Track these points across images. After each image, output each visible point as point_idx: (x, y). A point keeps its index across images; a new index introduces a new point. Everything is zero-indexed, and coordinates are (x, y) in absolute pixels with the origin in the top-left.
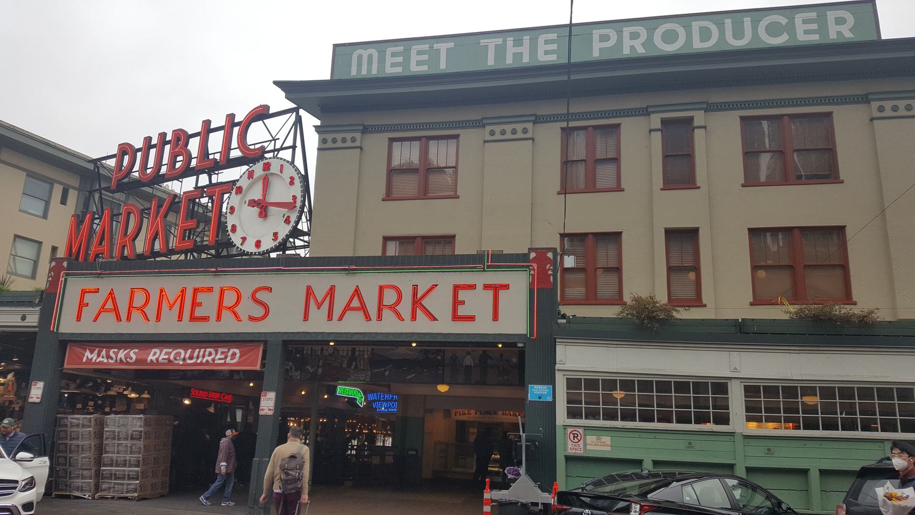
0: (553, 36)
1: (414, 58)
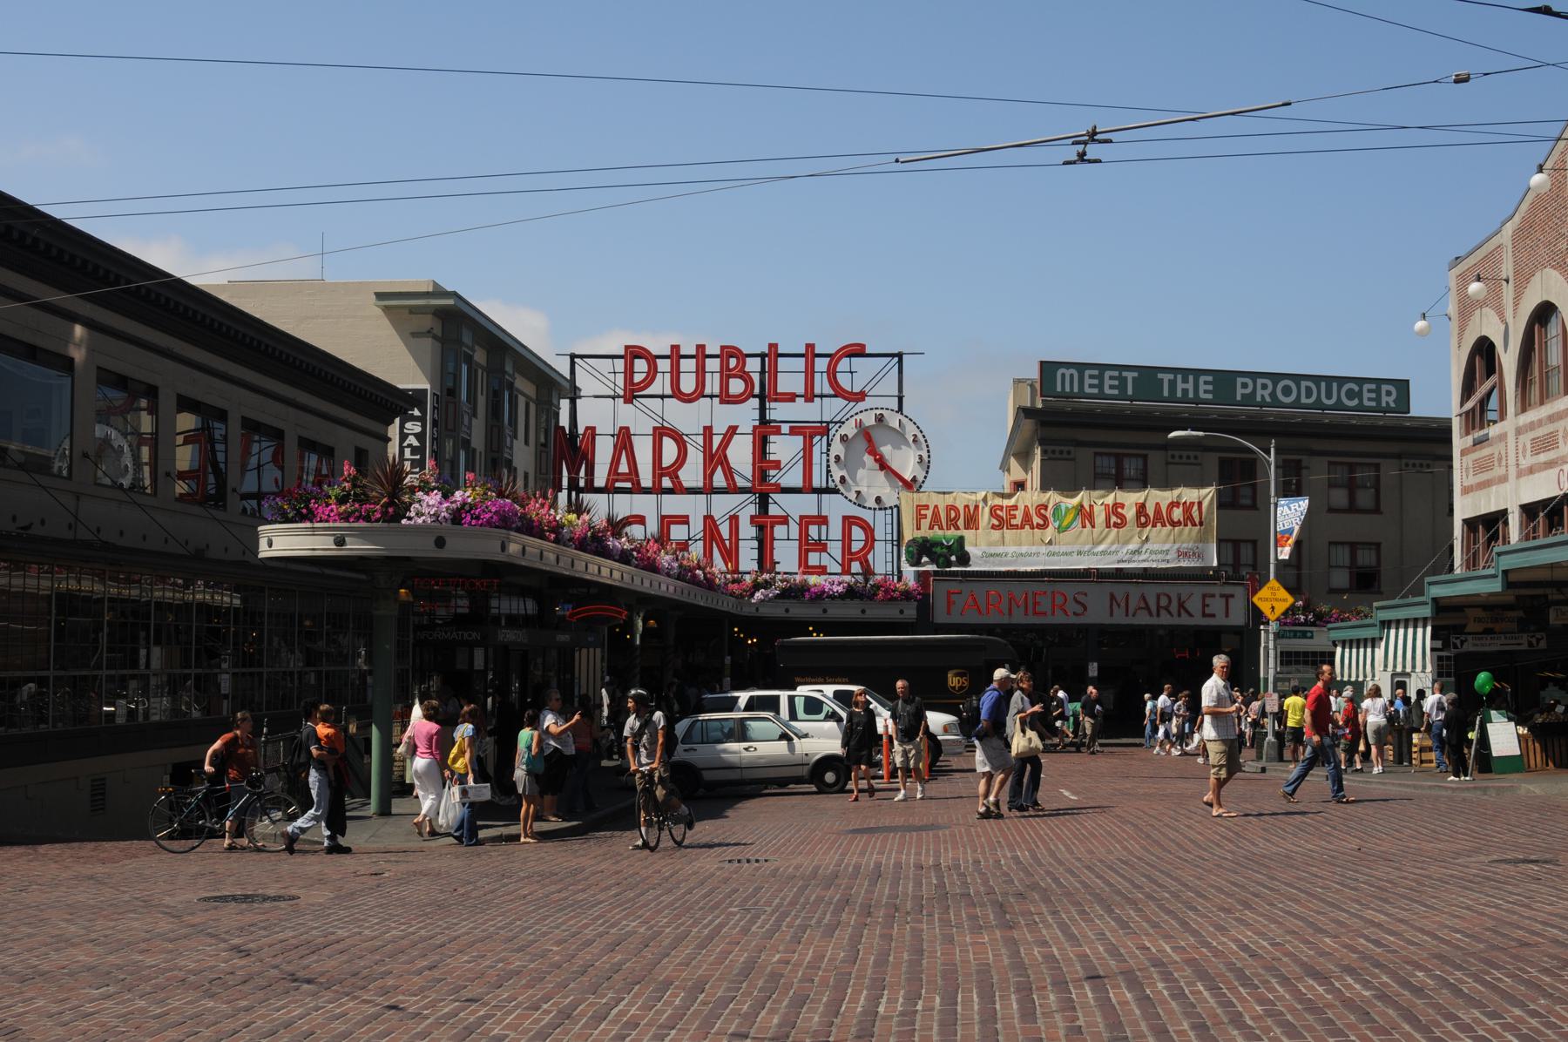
0: (1210, 378)
1: (1107, 382)
